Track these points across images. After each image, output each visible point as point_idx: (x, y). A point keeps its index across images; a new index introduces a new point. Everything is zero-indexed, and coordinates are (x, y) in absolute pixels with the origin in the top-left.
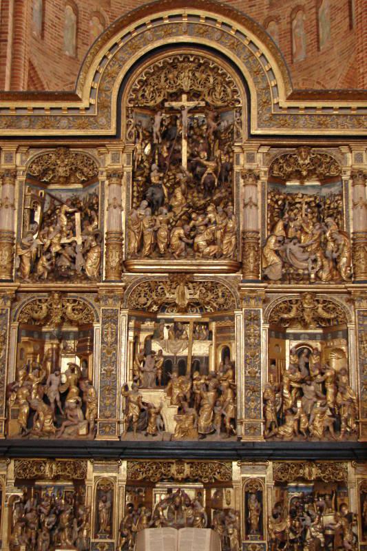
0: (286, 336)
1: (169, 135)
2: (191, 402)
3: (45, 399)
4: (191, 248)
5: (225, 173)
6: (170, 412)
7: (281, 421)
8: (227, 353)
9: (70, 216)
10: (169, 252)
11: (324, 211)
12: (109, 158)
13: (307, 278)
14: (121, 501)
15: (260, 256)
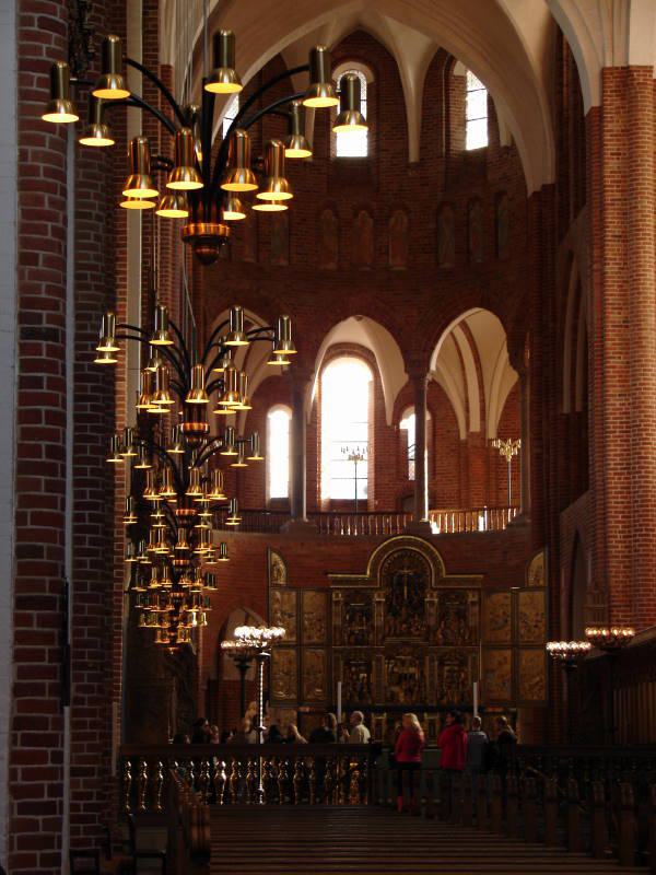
0: (444, 665)
1: (400, 584)
2: (409, 691)
3: (355, 689)
4: (410, 633)
5: (421, 603)
6: (402, 695)
7: (442, 698)
8: (422, 673)
9: (361, 620)
10: (402, 634)
11: (461, 615)
12: (376, 595)
13: (452, 644)
14: (384, 727)
15: (435, 635)
